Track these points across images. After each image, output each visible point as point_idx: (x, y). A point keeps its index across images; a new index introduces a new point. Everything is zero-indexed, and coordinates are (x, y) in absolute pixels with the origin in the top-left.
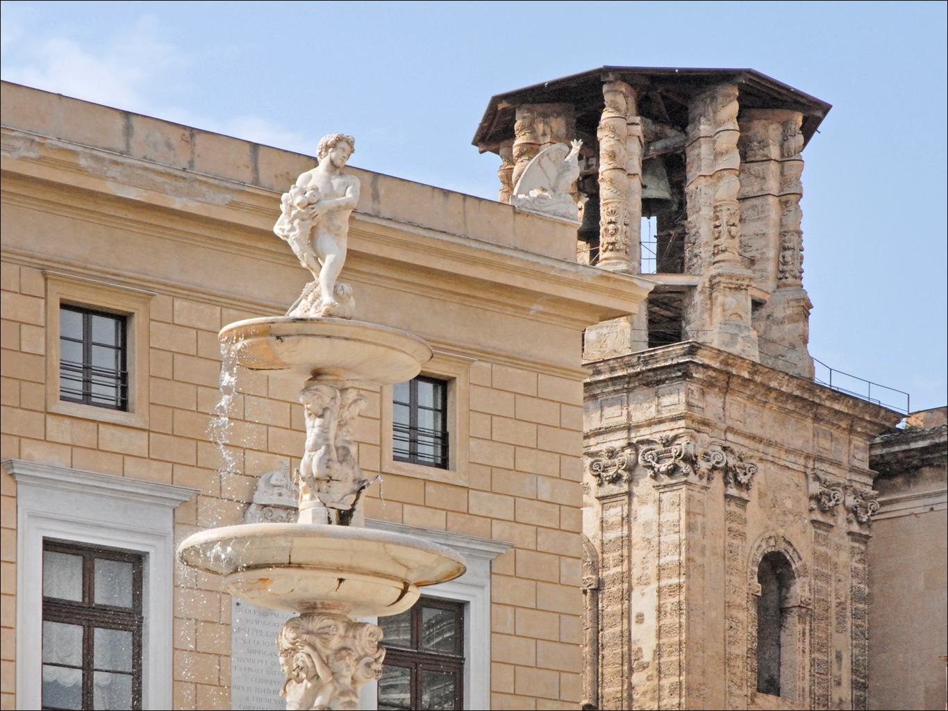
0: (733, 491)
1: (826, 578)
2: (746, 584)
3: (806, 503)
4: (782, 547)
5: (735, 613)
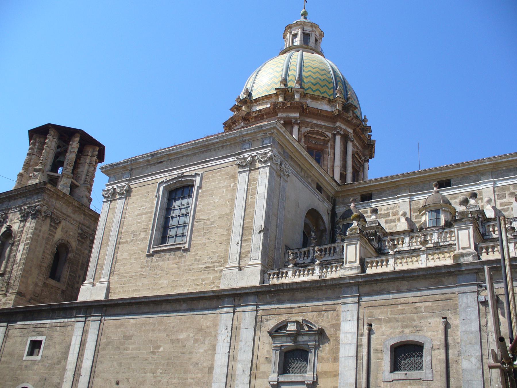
0: (53, 224)
1: (80, 255)
3: (77, 235)
4: (66, 243)
5: (46, 255)
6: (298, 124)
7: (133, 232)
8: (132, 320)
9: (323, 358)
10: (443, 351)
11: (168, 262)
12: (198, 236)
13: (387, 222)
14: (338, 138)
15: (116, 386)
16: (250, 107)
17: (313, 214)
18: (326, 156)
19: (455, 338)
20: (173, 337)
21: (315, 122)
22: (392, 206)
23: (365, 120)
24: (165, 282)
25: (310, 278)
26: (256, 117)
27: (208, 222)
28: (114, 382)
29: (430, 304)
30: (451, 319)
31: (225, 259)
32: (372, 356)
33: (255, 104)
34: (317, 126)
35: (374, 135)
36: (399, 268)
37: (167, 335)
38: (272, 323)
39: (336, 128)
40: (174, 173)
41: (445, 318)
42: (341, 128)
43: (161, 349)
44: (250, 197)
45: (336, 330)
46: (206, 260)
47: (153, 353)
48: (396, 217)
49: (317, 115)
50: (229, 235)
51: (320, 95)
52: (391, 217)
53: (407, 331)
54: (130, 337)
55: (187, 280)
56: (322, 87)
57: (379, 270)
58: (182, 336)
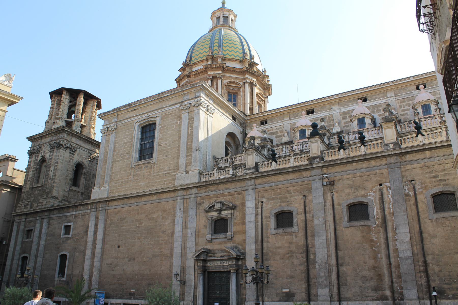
1: (91, 170)
2: (72, 167)
4: (81, 163)
6: (221, 78)
7: (122, 154)
8: (125, 209)
9: (236, 223)
10: (303, 215)
11: (144, 171)
12: (161, 154)
13: (277, 137)
14: (247, 85)
15: (118, 249)
16: (191, 69)
17: (231, 135)
18: (239, 97)
19: (311, 207)
20: (150, 217)
22: (279, 127)
23: (264, 71)
24: (143, 184)
25: (227, 176)
26: (195, 75)
27: (166, 146)
28: (117, 246)
29: (295, 188)
30: (308, 196)
31: (177, 168)
32: (264, 220)
33: (194, 66)
34: (233, 78)
35: (271, 81)
36: (278, 167)
37: (146, 216)
38: (206, 205)
39: (245, 79)
40: (144, 116)
41: (305, 196)
42: (248, 79)
43: (143, 224)
44: (190, 129)
45: (243, 206)
46: (166, 169)
47: (139, 227)
48: (282, 133)
49: (232, 71)
50: (179, 153)
51: (234, 58)
52: (279, 134)
53: (283, 204)
54: (124, 219)
55: (156, 182)
56: (235, 53)
58: (154, 216)
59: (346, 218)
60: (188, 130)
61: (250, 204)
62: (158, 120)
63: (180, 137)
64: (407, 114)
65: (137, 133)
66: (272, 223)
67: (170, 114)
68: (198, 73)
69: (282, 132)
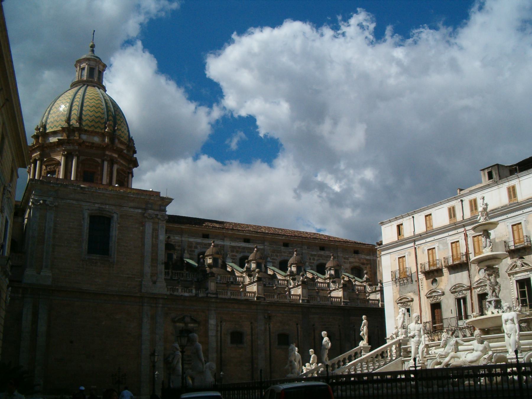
21: (121, 161)
25: (190, 294)
34: (122, 164)
40: (97, 205)
57: (223, 297)
59: (277, 343)
60: (153, 241)
61: (212, 322)
62: (115, 216)
63: (143, 245)
64: (275, 262)
65: (86, 223)
66: (228, 339)
67: (131, 216)
68: (92, 145)
69: (179, 246)
